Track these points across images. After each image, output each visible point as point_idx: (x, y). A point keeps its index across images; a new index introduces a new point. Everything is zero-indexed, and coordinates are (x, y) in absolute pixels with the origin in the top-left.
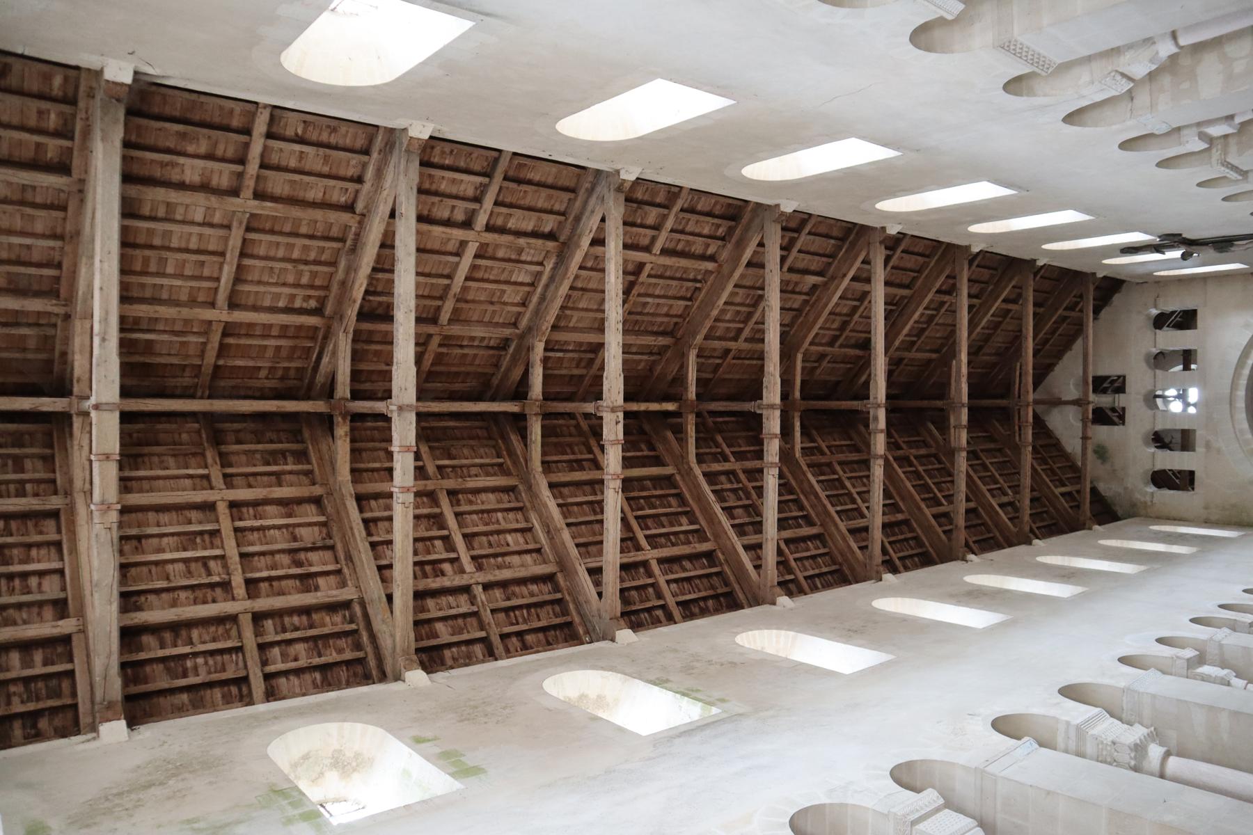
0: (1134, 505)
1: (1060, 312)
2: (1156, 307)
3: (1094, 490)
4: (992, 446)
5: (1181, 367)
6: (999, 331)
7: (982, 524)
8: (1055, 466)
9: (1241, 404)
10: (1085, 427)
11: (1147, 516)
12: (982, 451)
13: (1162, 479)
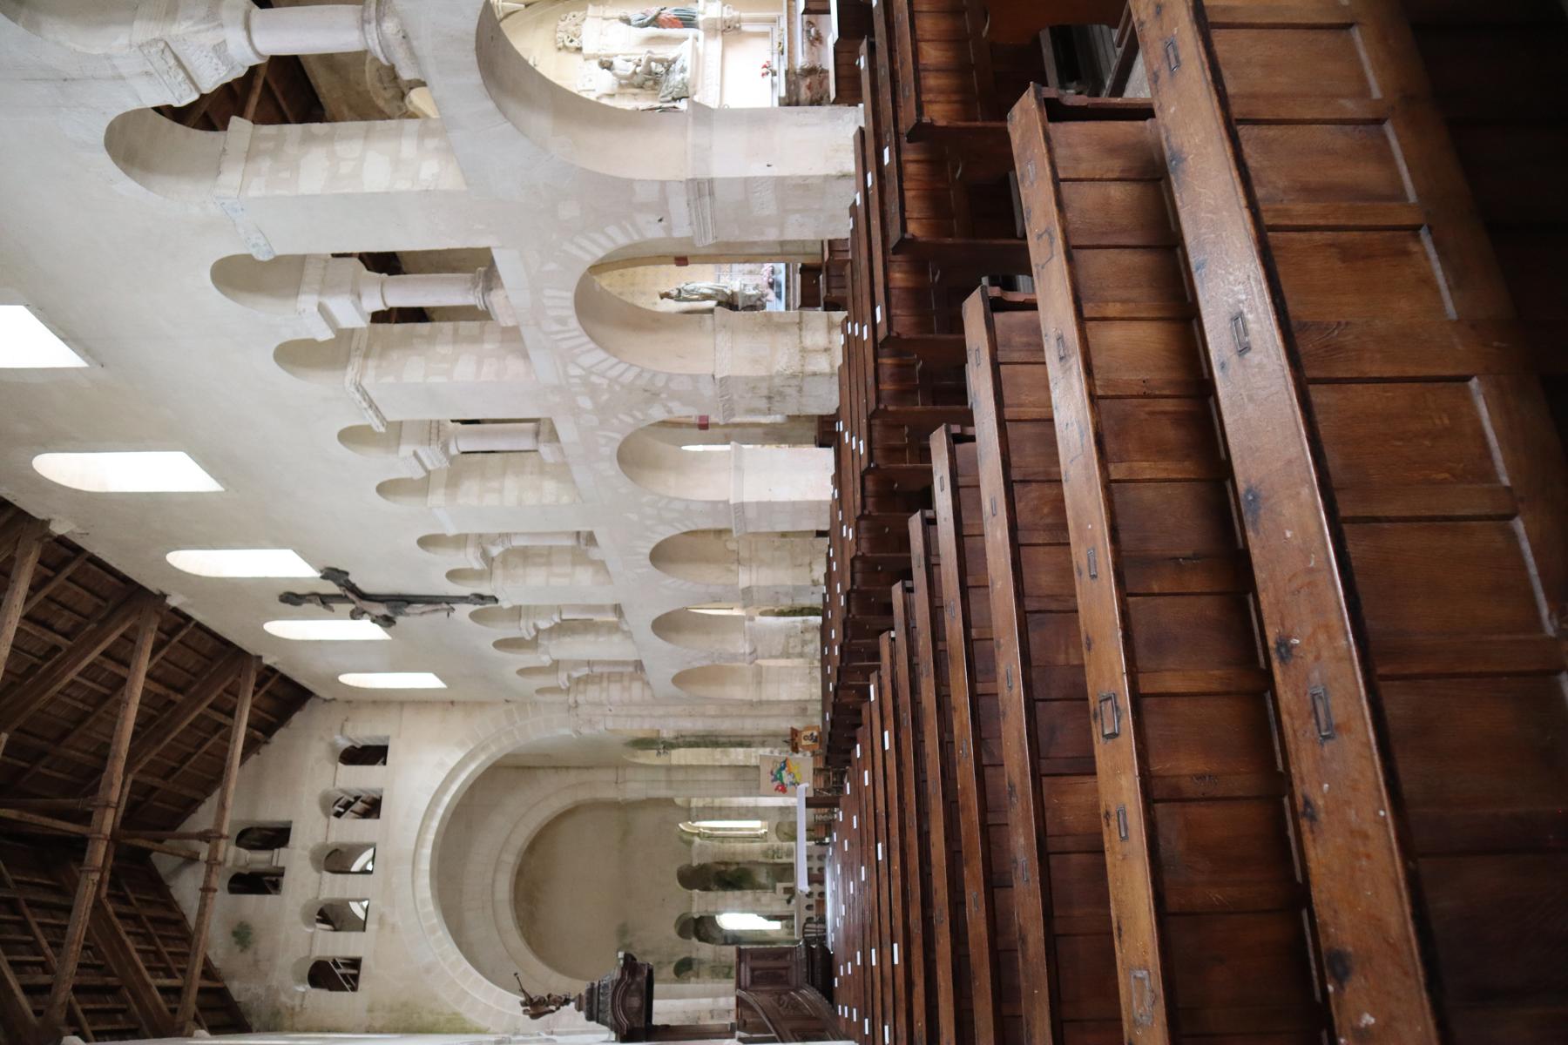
0: (276, 1013)
3: (207, 962)
8: (164, 950)
9: (425, 866)
13: (325, 975)
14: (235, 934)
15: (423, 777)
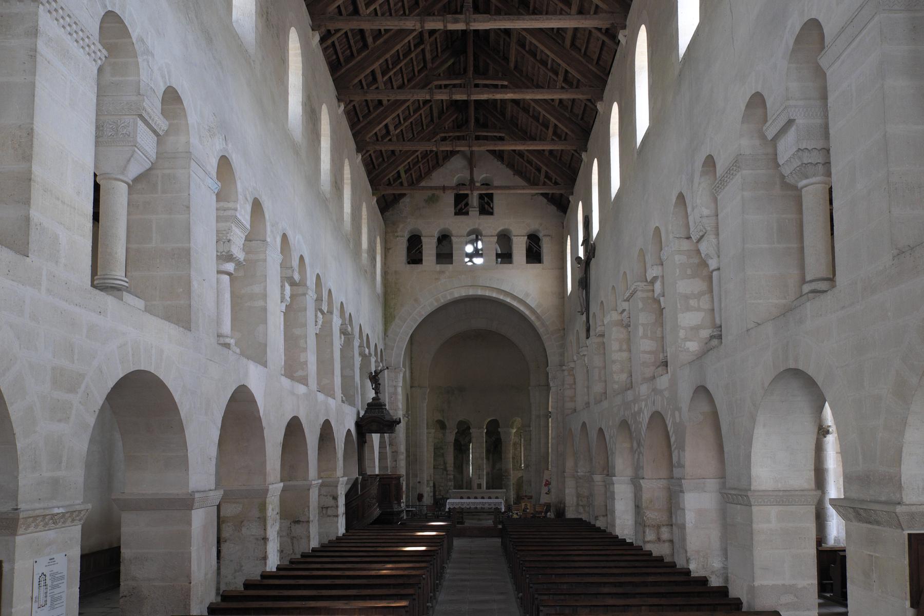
1: (544, 168)
3: (404, 195)
7: (369, 111)
8: (420, 164)
9: (471, 292)
10: (452, 188)
12: (431, 107)
13: (415, 242)
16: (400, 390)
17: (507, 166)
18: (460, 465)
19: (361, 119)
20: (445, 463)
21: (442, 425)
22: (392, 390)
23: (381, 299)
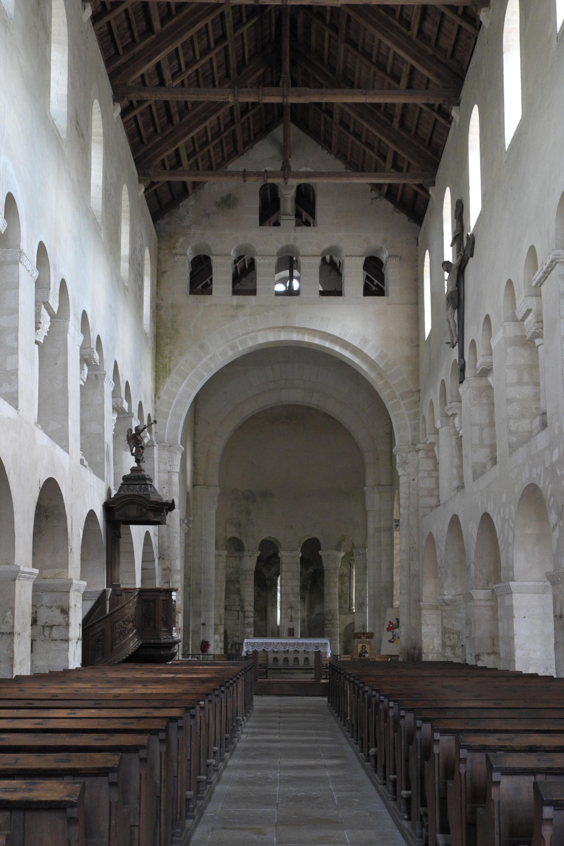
1: (393, 147)
2: (390, 256)
4: (233, 65)
5: (321, 289)
6: (374, 68)
7: (133, 40)
8: (210, 147)
9: (283, 336)
10: (258, 174)
11: (159, 248)
12: (226, 49)
14: (229, 196)
15: (352, 327)
16: (176, 478)
17: (337, 156)
18: (263, 608)
19: (121, 52)
20: (242, 600)
21: (236, 545)
22: (165, 477)
23: (150, 342)
